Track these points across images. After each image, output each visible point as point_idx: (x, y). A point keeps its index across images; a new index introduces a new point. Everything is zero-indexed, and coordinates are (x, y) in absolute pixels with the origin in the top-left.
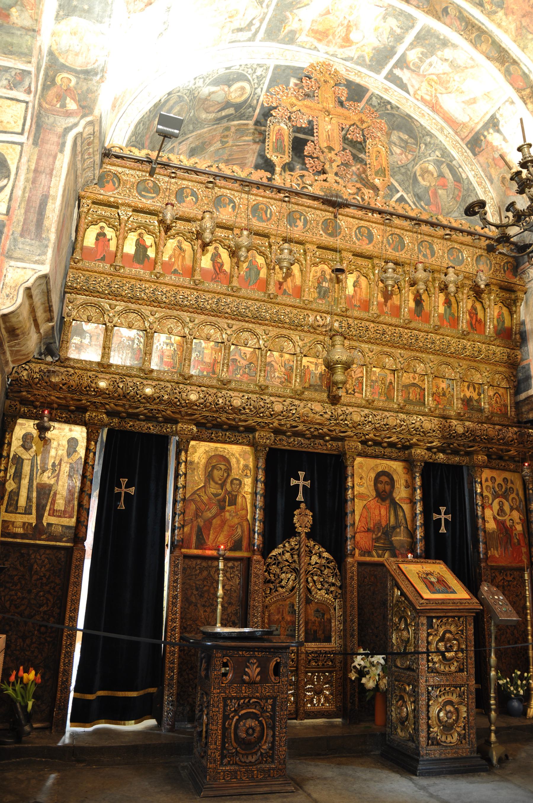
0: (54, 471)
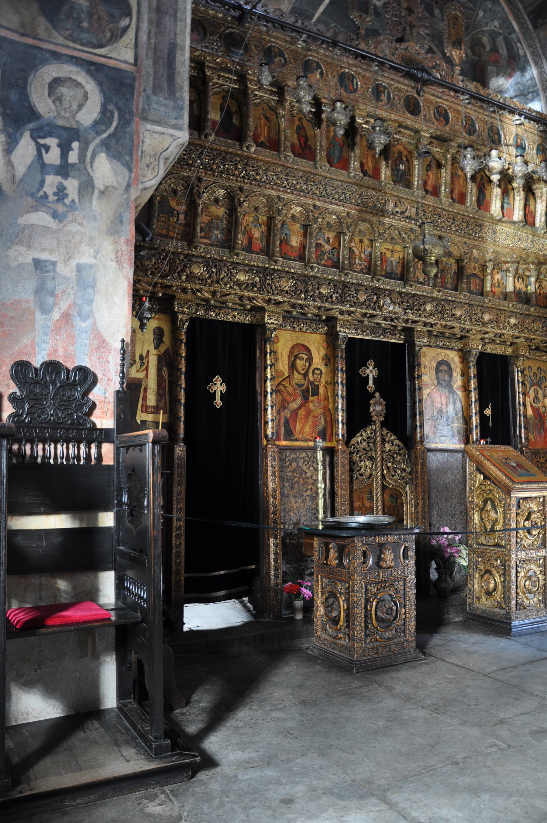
0: (142, 363)
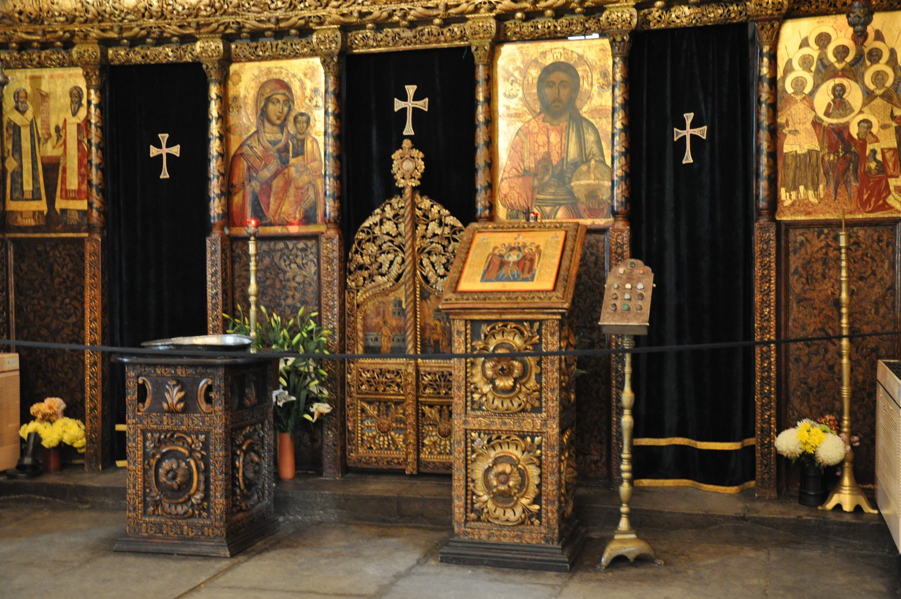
0: (59, 137)
